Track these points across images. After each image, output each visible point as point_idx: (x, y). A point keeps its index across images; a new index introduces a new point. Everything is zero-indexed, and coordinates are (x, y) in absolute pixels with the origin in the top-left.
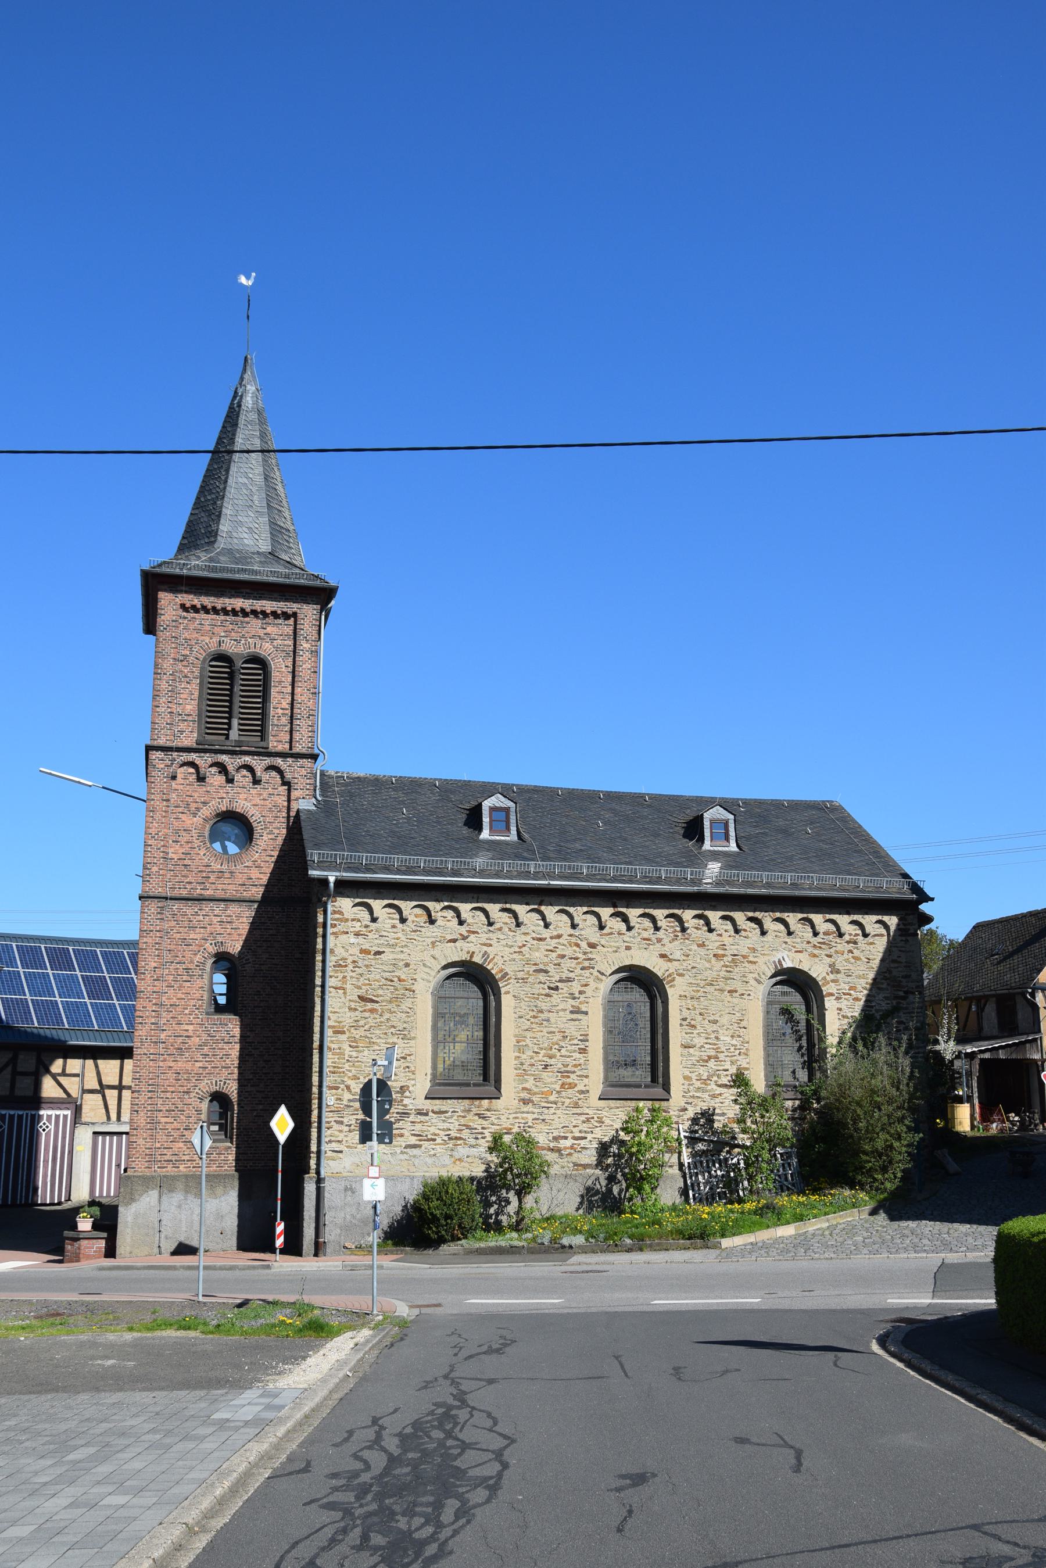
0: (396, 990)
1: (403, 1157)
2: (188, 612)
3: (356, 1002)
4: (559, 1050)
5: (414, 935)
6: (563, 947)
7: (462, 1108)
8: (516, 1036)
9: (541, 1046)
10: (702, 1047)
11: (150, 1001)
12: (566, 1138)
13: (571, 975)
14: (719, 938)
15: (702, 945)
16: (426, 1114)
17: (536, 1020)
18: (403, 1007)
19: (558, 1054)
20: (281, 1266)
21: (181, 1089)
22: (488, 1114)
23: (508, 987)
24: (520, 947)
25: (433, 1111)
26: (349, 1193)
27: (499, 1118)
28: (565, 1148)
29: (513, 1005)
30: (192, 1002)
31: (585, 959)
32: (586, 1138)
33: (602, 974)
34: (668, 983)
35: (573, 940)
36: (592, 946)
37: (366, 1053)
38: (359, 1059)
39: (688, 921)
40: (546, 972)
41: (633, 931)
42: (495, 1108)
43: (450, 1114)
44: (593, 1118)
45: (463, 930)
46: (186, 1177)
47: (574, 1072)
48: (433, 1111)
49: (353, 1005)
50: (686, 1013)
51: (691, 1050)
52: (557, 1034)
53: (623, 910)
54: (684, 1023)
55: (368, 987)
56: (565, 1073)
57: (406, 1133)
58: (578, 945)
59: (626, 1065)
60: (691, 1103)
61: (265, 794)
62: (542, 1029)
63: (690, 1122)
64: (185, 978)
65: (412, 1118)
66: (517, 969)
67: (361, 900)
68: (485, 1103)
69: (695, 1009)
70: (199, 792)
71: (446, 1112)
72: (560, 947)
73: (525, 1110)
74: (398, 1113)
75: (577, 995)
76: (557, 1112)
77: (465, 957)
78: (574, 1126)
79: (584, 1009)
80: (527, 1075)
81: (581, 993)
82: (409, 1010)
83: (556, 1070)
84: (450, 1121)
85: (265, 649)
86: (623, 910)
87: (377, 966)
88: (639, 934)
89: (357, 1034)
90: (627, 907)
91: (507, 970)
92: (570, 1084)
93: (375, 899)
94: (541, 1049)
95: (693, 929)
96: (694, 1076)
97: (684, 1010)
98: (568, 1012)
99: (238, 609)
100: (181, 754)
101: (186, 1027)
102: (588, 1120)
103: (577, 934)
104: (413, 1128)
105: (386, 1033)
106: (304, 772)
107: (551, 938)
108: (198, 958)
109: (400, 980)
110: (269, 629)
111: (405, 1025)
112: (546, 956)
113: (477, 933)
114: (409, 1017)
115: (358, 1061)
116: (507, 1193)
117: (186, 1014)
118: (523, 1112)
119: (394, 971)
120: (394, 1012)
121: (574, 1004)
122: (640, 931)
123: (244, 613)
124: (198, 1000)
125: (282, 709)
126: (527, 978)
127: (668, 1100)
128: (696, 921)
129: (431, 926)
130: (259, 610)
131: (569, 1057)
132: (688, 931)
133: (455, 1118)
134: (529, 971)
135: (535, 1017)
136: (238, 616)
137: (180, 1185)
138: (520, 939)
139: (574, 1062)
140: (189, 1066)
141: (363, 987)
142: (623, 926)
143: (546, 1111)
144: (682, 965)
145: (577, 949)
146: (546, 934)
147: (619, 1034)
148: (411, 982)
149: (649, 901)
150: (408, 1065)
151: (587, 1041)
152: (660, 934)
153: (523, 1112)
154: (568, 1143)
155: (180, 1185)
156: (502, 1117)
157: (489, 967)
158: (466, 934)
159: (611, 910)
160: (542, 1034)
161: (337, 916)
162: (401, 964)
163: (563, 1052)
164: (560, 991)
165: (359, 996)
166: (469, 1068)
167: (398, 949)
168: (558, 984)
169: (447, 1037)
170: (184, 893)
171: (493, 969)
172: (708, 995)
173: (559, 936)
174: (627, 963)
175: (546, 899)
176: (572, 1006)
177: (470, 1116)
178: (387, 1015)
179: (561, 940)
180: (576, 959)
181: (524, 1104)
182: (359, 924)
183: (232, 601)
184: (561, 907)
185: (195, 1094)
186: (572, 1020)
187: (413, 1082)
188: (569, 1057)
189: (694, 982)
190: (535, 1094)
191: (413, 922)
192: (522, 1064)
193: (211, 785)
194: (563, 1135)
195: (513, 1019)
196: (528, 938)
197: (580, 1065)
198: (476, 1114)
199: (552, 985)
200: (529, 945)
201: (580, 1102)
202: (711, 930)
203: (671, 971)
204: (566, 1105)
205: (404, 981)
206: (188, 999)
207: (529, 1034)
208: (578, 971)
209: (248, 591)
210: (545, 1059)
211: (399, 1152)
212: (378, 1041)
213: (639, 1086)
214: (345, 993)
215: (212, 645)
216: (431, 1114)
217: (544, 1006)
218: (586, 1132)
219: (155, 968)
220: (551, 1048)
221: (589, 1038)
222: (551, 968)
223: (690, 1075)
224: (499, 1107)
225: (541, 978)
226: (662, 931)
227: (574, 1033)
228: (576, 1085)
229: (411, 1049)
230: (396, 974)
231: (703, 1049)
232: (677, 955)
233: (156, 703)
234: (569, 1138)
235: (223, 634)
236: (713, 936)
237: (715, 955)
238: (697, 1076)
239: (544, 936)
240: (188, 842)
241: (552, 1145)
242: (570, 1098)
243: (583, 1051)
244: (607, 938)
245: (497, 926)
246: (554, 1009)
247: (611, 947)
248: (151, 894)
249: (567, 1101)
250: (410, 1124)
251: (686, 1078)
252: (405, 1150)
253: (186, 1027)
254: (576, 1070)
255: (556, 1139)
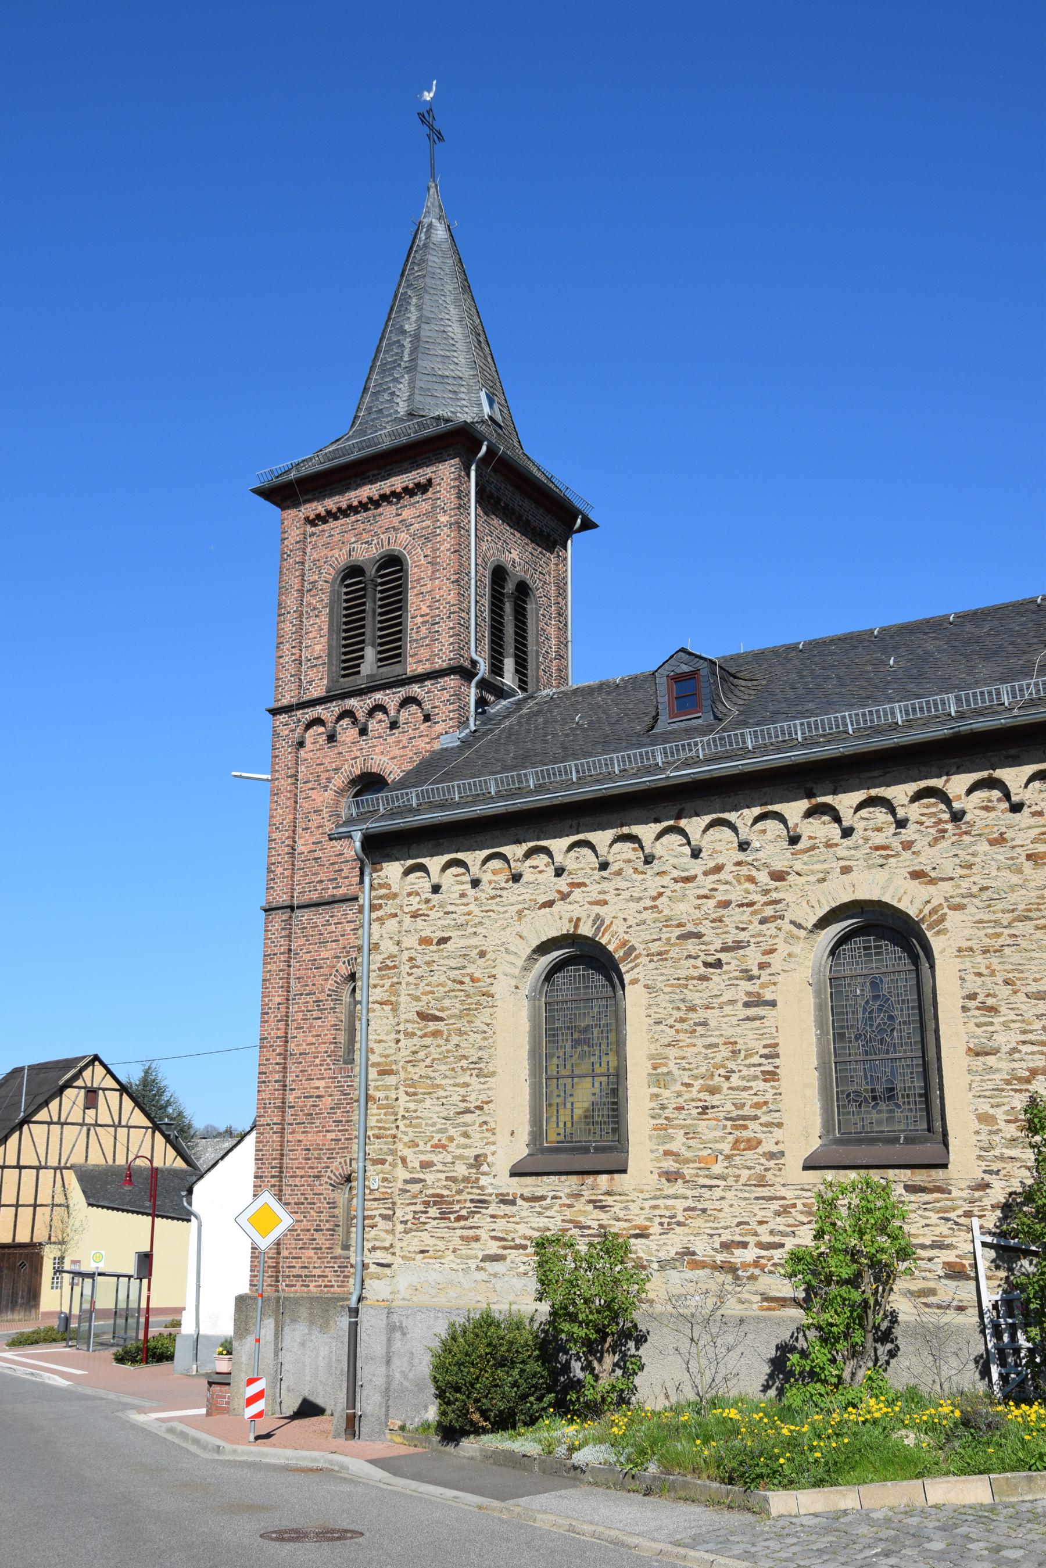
0: (468, 996)
1: (481, 1276)
2: (316, 525)
3: (414, 1022)
4: (727, 1078)
5: (492, 905)
6: (727, 887)
7: (567, 1191)
8: (651, 1057)
9: (695, 1072)
10: (1014, 1050)
11: (274, 1051)
12: (744, 1245)
13: (743, 936)
14: (1037, 819)
15: (1000, 840)
16: (513, 1203)
17: (685, 1026)
18: (478, 1023)
19: (726, 1085)
20: (235, 1451)
21: (311, 1172)
22: (609, 1200)
23: (636, 970)
24: (654, 899)
25: (522, 1197)
26: (398, 1335)
27: (626, 1208)
28: (745, 1266)
29: (645, 1002)
30: (323, 1048)
31: (766, 904)
32: (782, 1245)
33: (799, 926)
34: (931, 927)
35: (744, 871)
36: (778, 876)
37: (428, 1103)
38: (418, 1114)
39: (959, 797)
40: (699, 936)
41: (854, 837)
42: (620, 1190)
43: (549, 1201)
44: (794, 1206)
45: (562, 883)
46: (312, 1299)
47: (756, 1118)
48: (522, 1197)
49: (410, 1027)
50: (973, 984)
51: (991, 1060)
52: (722, 1048)
53: (828, 799)
54: (972, 1004)
55: (430, 997)
56: (739, 1121)
57: (484, 1235)
58: (752, 880)
59: (874, 1098)
60: (997, 1172)
61: (405, 741)
62: (694, 1041)
63: (999, 1213)
64: (315, 1014)
65: (493, 1209)
66: (650, 938)
67: (414, 861)
68: (603, 1179)
69: (993, 973)
70: (329, 756)
71: (543, 1198)
72: (721, 887)
73: (671, 1191)
74: (472, 1201)
75: (755, 972)
76: (729, 1195)
77: (566, 928)
78: (761, 1223)
79: (768, 996)
80: (673, 1127)
81: (762, 966)
82: (485, 1028)
83: (722, 1115)
84: (548, 1214)
85: (401, 542)
86: (828, 799)
87: (442, 962)
88: (866, 840)
89: (416, 1072)
90: (835, 793)
91: (634, 942)
92: (749, 1140)
93: (432, 856)
94: (696, 1078)
95: (977, 812)
96: (1000, 1114)
97: (971, 978)
98: (740, 1004)
99: (365, 500)
100: (306, 711)
101: (317, 1083)
102: (784, 1211)
103: (749, 859)
104: (494, 1226)
105: (453, 1069)
106: (446, 695)
107: (706, 873)
108: (330, 985)
109: (473, 981)
110: (406, 513)
111: (480, 1053)
112: (698, 907)
113: (584, 885)
114: (485, 1039)
115: (418, 1117)
116: (637, 1349)
117: (317, 1065)
118: (668, 1197)
119: (464, 967)
120: (466, 1033)
121: (751, 989)
122: (869, 833)
123: (375, 503)
124: (331, 1043)
125: (422, 616)
126: (667, 952)
127: (945, 1166)
128: (979, 795)
129: (516, 886)
130: (388, 492)
131: (745, 1089)
132: (968, 818)
133: (557, 1208)
134: (669, 939)
135: (682, 1020)
136: (369, 509)
137: (303, 1312)
138: (654, 884)
139: (756, 1099)
140: (319, 1139)
141: (424, 998)
142: (835, 831)
143: (707, 1194)
144: (959, 886)
145: (751, 887)
146: (696, 867)
147: (857, 1039)
148: (489, 981)
149: (875, 773)
150: (484, 1118)
151: (777, 1056)
152: (909, 833)
153: (668, 1197)
154: (749, 1255)
155: (303, 1312)
156: (632, 1206)
157: (603, 941)
158: (565, 889)
159: (803, 805)
160: (695, 1050)
161: (383, 891)
162: (474, 953)
163: (735, 1080)
164: (725, 968)
165: (418, 1013)
166: (596, 1119)
167: (470, 930)
168: (722, 956)
169: (561, 1068)
170: (314, 896)
171: (609, 942)
172: (1020, 941)
173: (718, 869)
174: (846, 898)
175: (688, 806)
176: (749, 994)
177: (580, 1205)
178: (455, 1039)
179: (723, 876)
180: (751, 904)
181: (668, 1180)
182: (418, 899)
183: (358, 492)
184: (714, 816)
185: (326, 1179)
186: (748, 1019)
187: (493, 1148)
188: (745, 1089)
189: (986, 917)
190: (687, 1161)
191: (490, 882)
192: (663, 1108)
193: (344, 743)
194: (738, 1238)
195: (646, 1027)
196: (666, 880)
197: (766, 1103)
198: (590, 1201)
199: (710, 959)
200: (668, 893)
201: (769, 1175)
202: (1017, 808)
203: (935, 903)
204: (743, 1180)
205: (478, 980)
206: (319, 1044)
207: (672, 1053)
208: (755, 927)
209: (375, 472)
210: (702, 1096)
211: (473, 1267)
212: (443, 1082)
213: (895, 1140)
214: (394, 1010)
215: (340, 558)
216: (519, 1201)
217: (697, 999)
218: (782, 1234)
219: (279, 1004)
220: (712, 1076)
221: (780, 1050)
222: (706, 928)
223: (991, 1111)
224: (626, 1188)
225: (690, 947)
226: (912, 827)
227: (753, 1044)
228: (760, 1142)
229: (490, 1093)
230: (468, 971)
231: (1017, 1056)
232: (948, 867)
233: (280, 653)
234: (751, 1245)
235: (353, 540)
236: (1023, 818)
237: (1029, 857)
238: (1007, 1113)
239: (692, 873)
240: (318, 827)
241: (719, 1258)
242: (749, 1168)
243: (771, 1076)
244: (805, 857)
245: (613, 868)
246: (716, 1002)
247: (813, 872)
248: (274, 905)
249: (745, 1174)
250: (489, 1220)
251: (984, 1118)
252: (482, 1264)
253: (317, 1083)
254: (759, 1113)
255: (726, 1246)
